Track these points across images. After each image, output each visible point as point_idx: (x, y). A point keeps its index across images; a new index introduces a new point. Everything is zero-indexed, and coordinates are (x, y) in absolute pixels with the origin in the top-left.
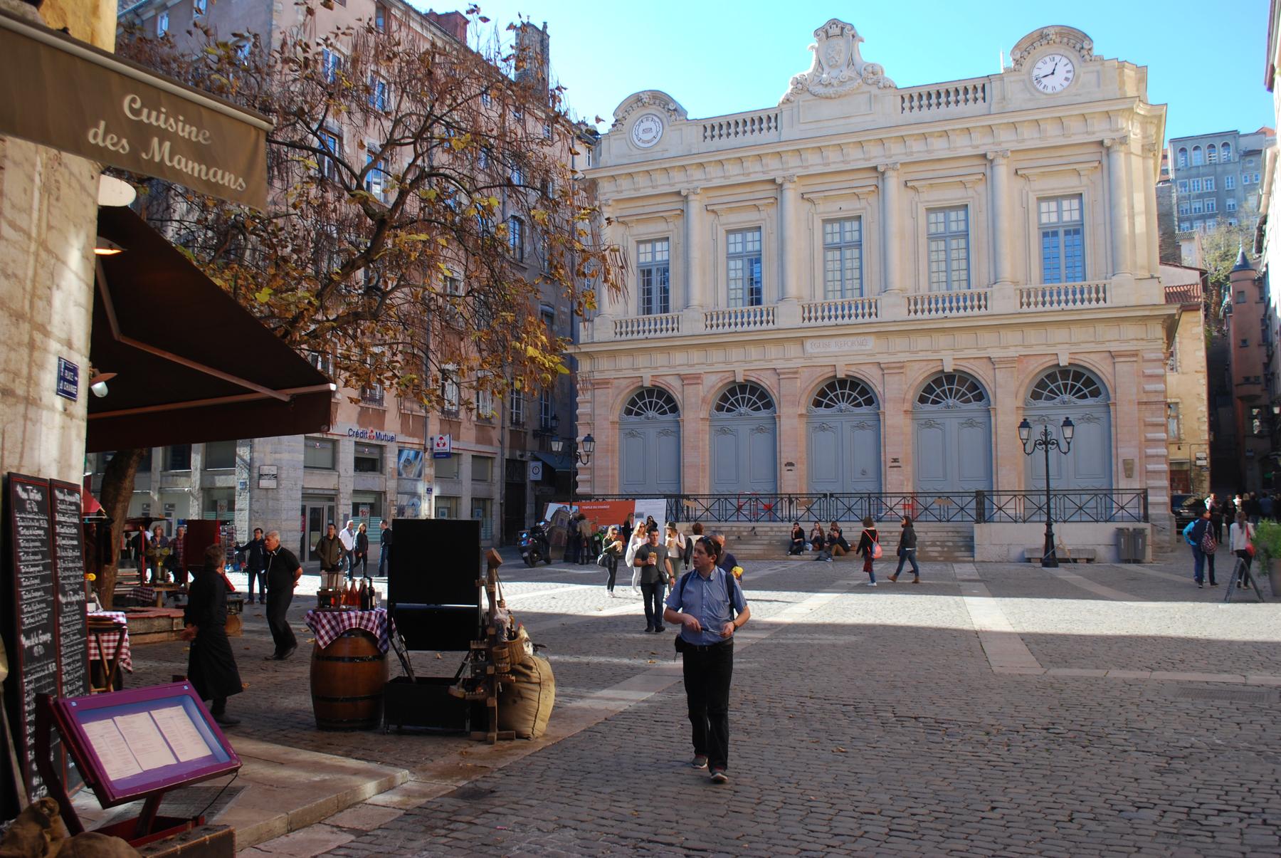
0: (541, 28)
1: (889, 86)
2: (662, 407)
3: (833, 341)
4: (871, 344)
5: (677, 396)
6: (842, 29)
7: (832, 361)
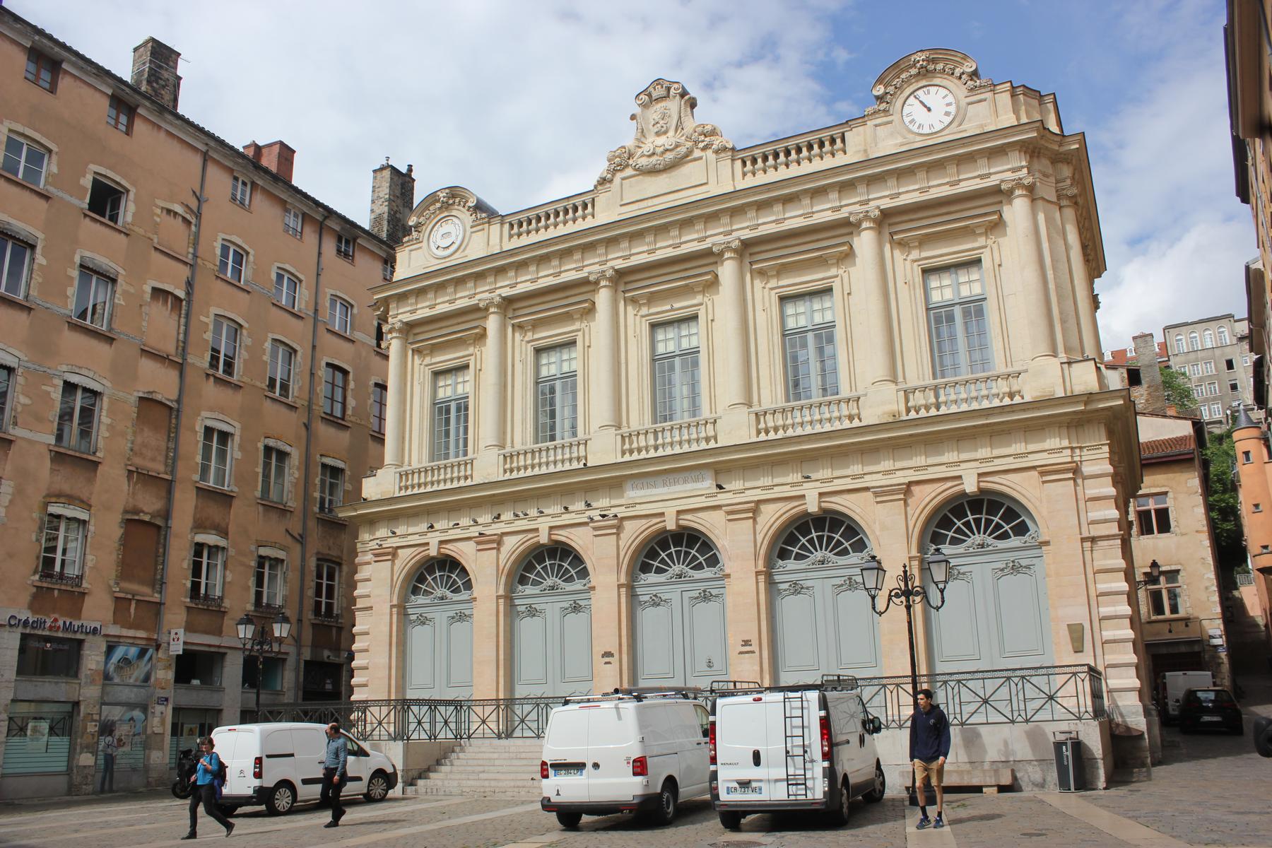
0: (404, 170)
6: (669, 89)
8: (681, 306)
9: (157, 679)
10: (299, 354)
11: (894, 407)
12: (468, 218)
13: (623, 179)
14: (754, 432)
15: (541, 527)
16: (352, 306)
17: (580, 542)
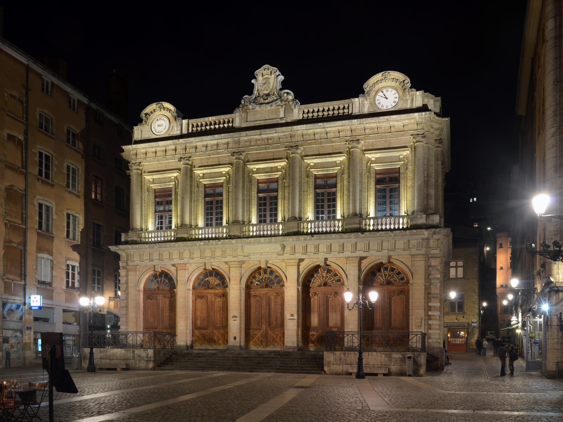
9: (25, 319)
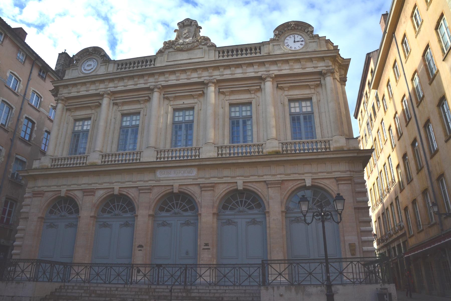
1: (214, 46)
2: (71, 209)
3: (172, 171)
4: (194, 173)
5: (79, 202)
6: (191, 22)
7: (171, 183)
8: (188, 102)
10: (14, 110)
11: (277, 149)
12: (100, 60)
13: (169, 52)
14: (217, 155)
15: (115, 187)
16: (41, 98)
17: (133, 195)
